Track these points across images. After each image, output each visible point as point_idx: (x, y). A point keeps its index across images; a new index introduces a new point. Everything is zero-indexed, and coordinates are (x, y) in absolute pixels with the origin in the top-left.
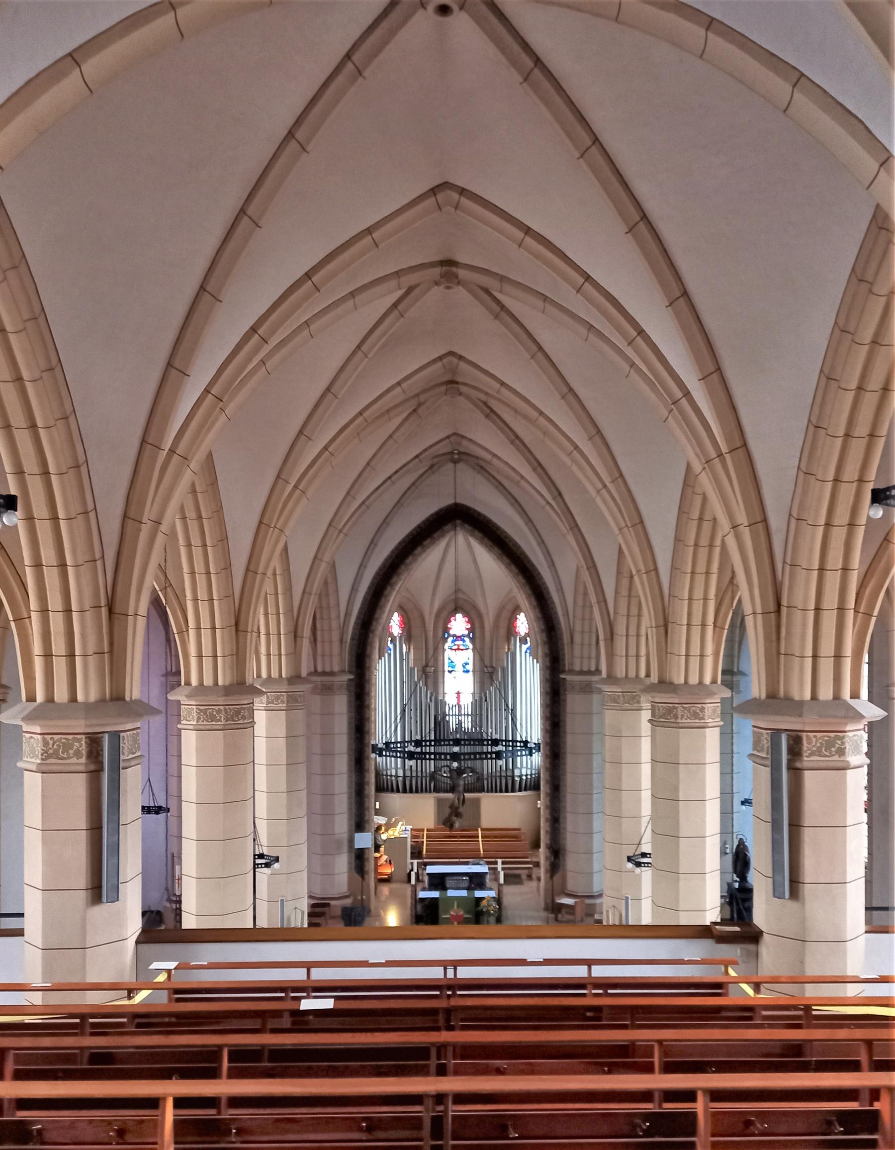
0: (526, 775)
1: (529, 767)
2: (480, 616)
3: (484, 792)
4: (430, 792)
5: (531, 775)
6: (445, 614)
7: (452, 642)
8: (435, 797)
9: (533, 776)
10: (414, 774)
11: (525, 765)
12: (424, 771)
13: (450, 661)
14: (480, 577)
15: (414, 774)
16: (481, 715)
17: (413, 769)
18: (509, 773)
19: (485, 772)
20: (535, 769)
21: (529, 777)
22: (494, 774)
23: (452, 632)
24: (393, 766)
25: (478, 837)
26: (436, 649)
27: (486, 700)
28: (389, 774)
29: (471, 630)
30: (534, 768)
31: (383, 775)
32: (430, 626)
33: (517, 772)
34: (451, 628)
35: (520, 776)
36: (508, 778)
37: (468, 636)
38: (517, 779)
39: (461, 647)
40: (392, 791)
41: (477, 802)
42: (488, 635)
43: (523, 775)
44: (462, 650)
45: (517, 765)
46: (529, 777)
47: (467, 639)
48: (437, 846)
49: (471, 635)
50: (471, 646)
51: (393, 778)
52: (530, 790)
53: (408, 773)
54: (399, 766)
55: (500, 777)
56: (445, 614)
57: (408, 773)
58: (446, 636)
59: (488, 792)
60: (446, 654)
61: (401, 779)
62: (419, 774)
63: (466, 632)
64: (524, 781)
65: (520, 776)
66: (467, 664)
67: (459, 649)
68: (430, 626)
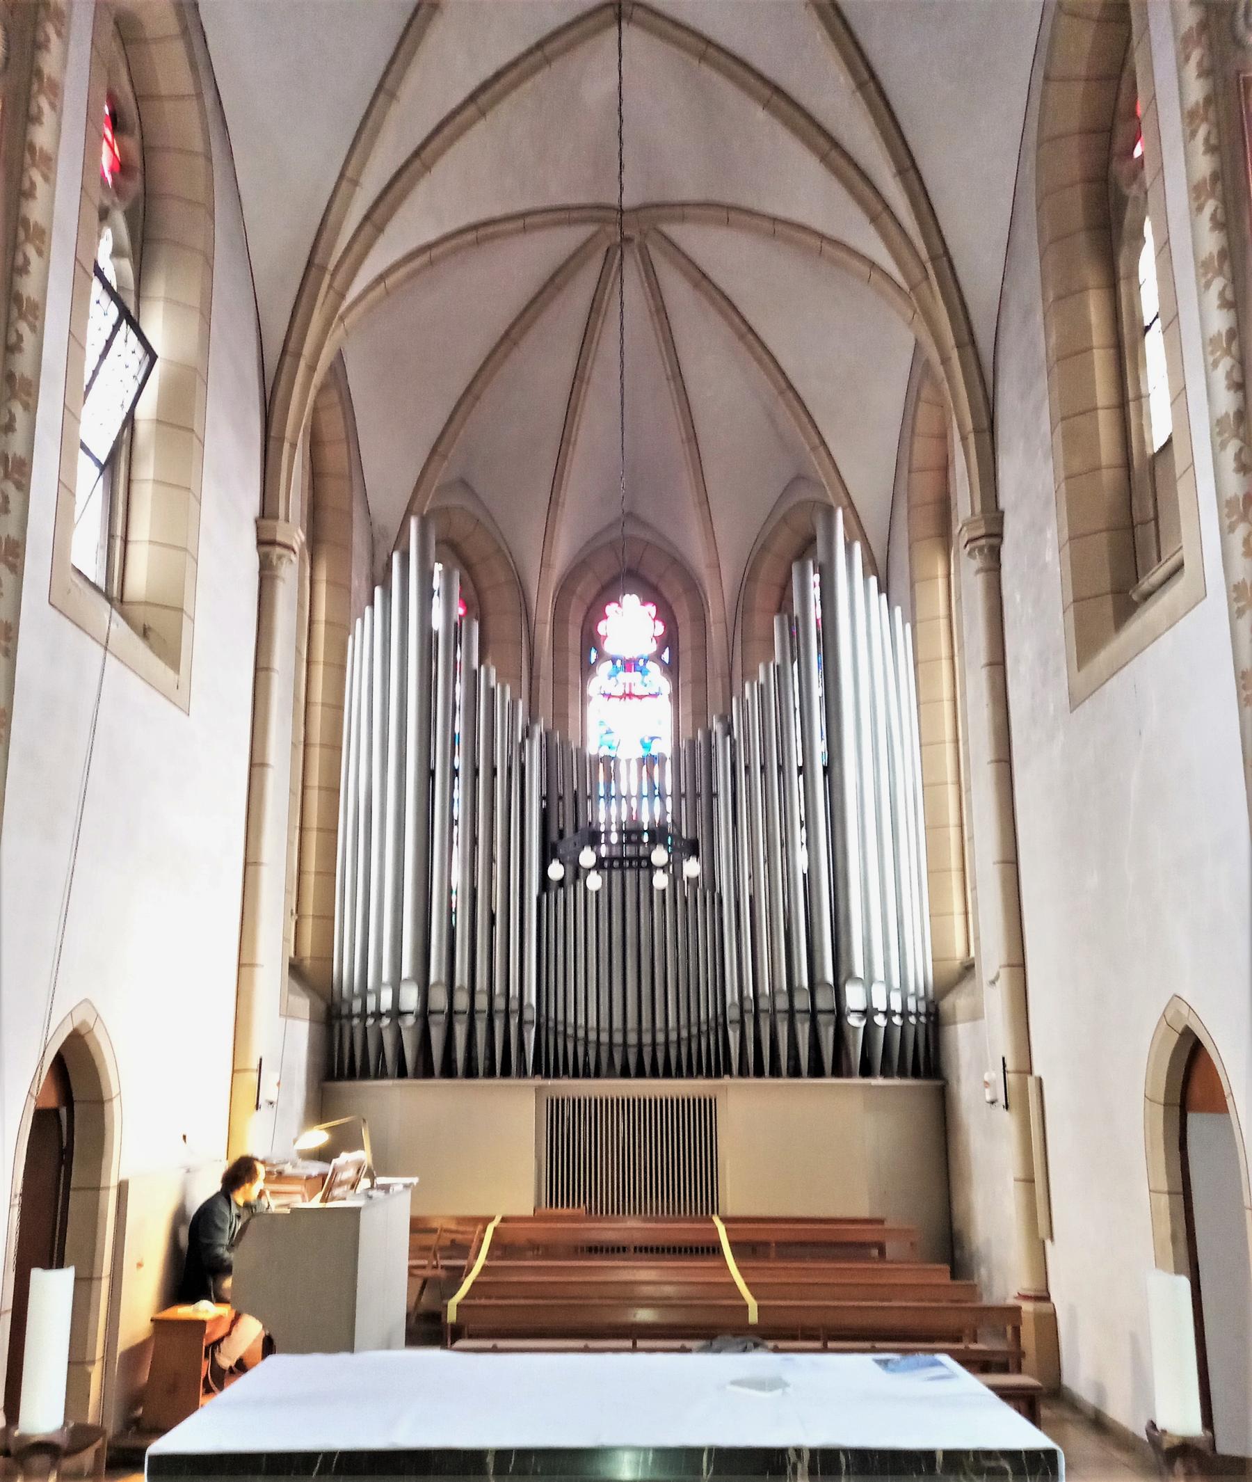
0: (888, 1013)
1: (896, 983)
2: (693, 587)
3: (731, 1075)
4: (523, 1073)
5: (904, 1014)
6: (587, 588)
7: (610, 677)
8: (538, 1090)
9: (912, 1020)
10: (462, 1002)
11: (879, 973)
12: (498, 988)
13: (603, 730)
14: (693, 438)
15: (462, 1002)
16: (712, 795)
17: (458, 983)
18: (825, 1000)
19: (732, 996)
20: (916, 994)
21: (897, 1020)
22: (764, 1004)
23: (609, 647)
24: (386, 977)
25: (716, 1250)
26: (560, 682)
27: (728, 731)
28: (371, 1006)
29: (669, 640)
30: (912, 989)
31: (350, 1016)
32: (544, 611)
33: (854, 997)
34: (606, 637)
35: (868, 1013)
36: (821, 1018)
37: (657, 657)
38: (853, 1020)
39: (637, 691)
40: (381, 1074)
41: (705, 1110)
42: (716, 633)
43: (876, 1012)
44: (640, 697)
45: (851, 976)
46: (897, 1020)
47: (653, 668)
48: (529, 1271)
49: (666, 656)
50: (665, 686)
51: (386, 1022)
52: (902, 1073)
53: (439, 1000)
54: (406, 971)
55: (791, 1012)
56: (587, 588)
57: (439, 1000)
58: (593, 659)
59: (743, 1073)
60: (592, 709)
61: (410, 1020)
62: (482, 1002)
63: (653, 647)
64: (882, 1031)
65: (868, 1013)
66: (652, 739)
67: (630, 695)
68: (544, 611)
